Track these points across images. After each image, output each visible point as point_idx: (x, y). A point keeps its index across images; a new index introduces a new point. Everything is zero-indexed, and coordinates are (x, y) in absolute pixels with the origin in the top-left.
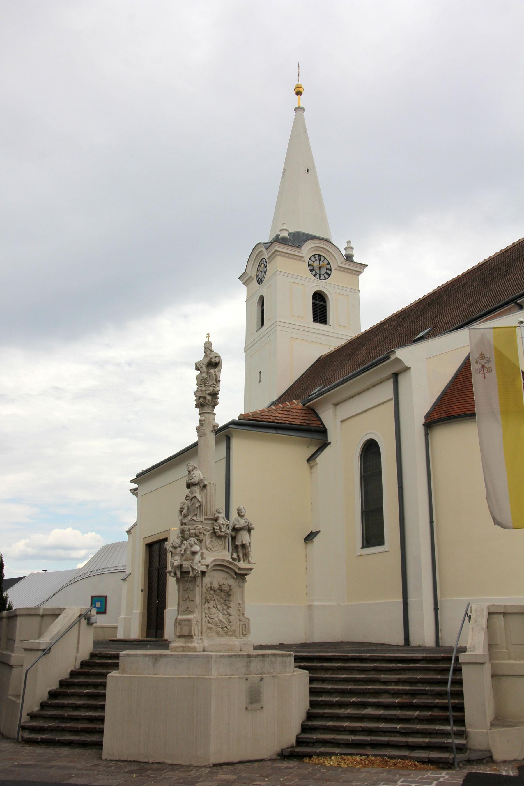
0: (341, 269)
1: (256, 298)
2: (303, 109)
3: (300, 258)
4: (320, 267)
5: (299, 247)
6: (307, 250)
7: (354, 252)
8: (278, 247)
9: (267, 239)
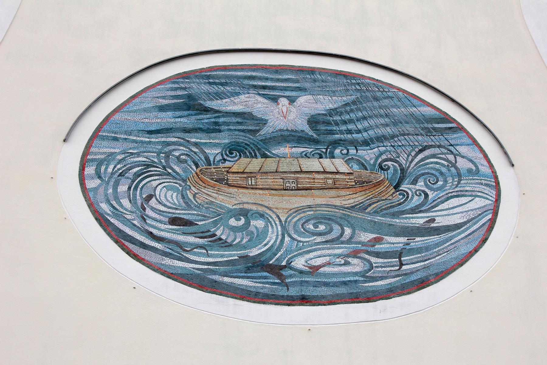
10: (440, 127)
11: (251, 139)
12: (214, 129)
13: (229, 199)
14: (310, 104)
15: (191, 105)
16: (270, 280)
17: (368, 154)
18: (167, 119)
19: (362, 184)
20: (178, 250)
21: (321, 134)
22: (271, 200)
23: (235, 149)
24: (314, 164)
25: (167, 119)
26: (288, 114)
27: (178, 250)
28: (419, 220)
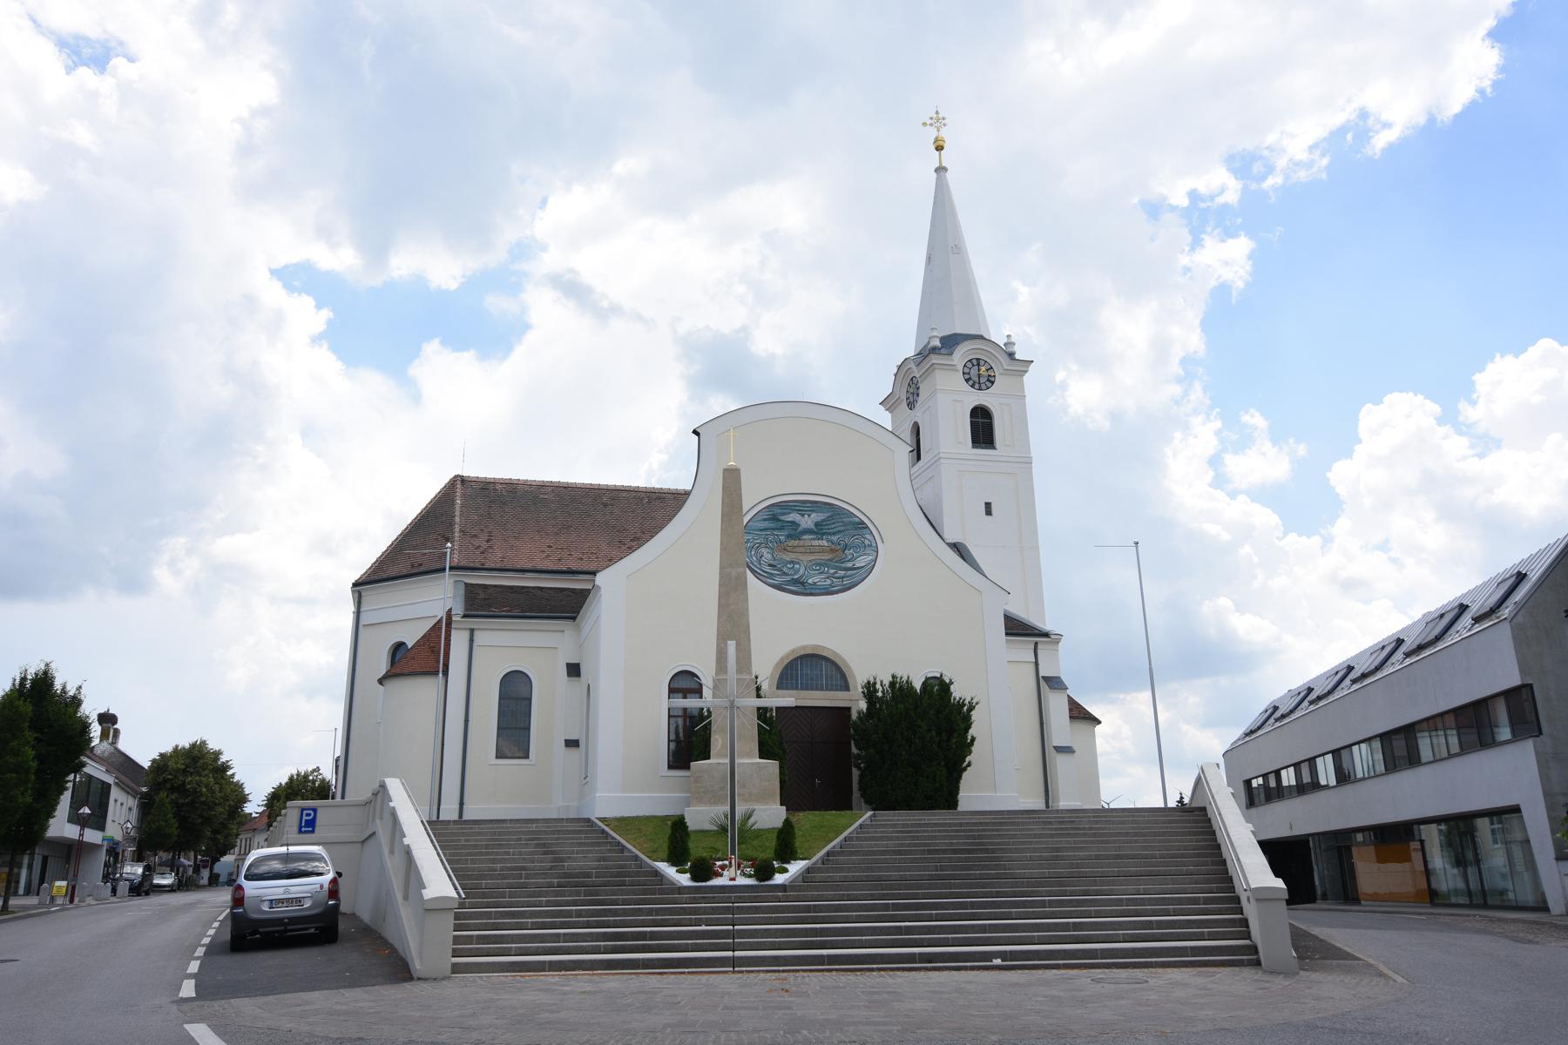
0: (1007, 372)
1: (908, 426)
2: (945, 169)
3: (952, 367)
4: (979, 375)
5: (951, 354)
6: (961, 355)
7: (1016, 349)
8: (935, 359)
9: (910, 352)
10: (861, 526)
11: (795, 532)
12: (781, 529)
13: (788, 557)
14: (817, 516)
15: (774, 518)
16: (801, 588)
17: (834, 538)
18: (766, 524)
19: (832, 551)
20: (771, 576)
21: (819, 530)
22: (801, 557)
23: (789, 537)
24: (816, 543)
25: (766, 524)
26: (807, 522)
27: (771, 576)
28: (850, 565)
